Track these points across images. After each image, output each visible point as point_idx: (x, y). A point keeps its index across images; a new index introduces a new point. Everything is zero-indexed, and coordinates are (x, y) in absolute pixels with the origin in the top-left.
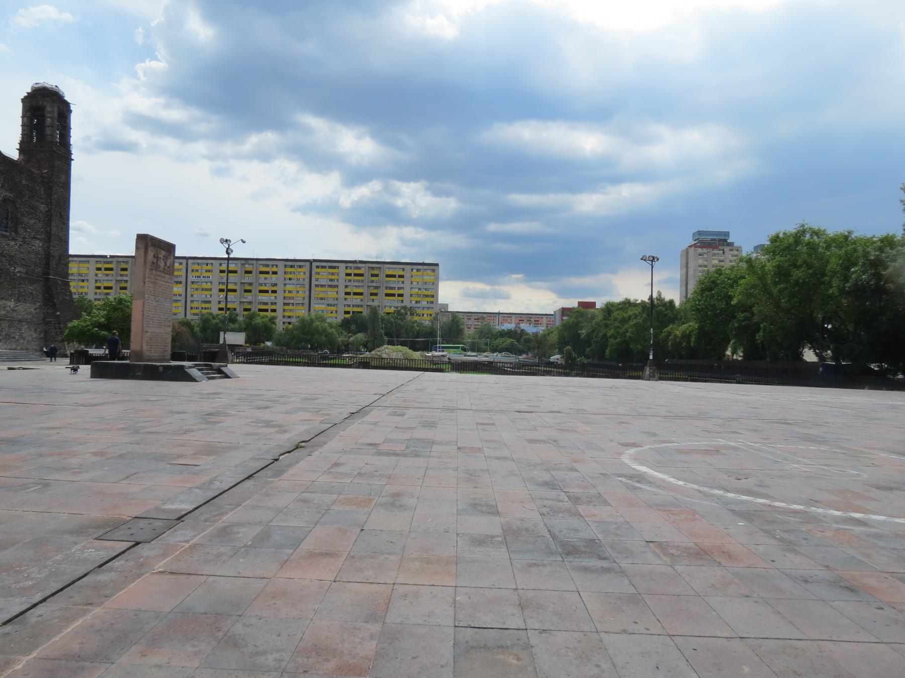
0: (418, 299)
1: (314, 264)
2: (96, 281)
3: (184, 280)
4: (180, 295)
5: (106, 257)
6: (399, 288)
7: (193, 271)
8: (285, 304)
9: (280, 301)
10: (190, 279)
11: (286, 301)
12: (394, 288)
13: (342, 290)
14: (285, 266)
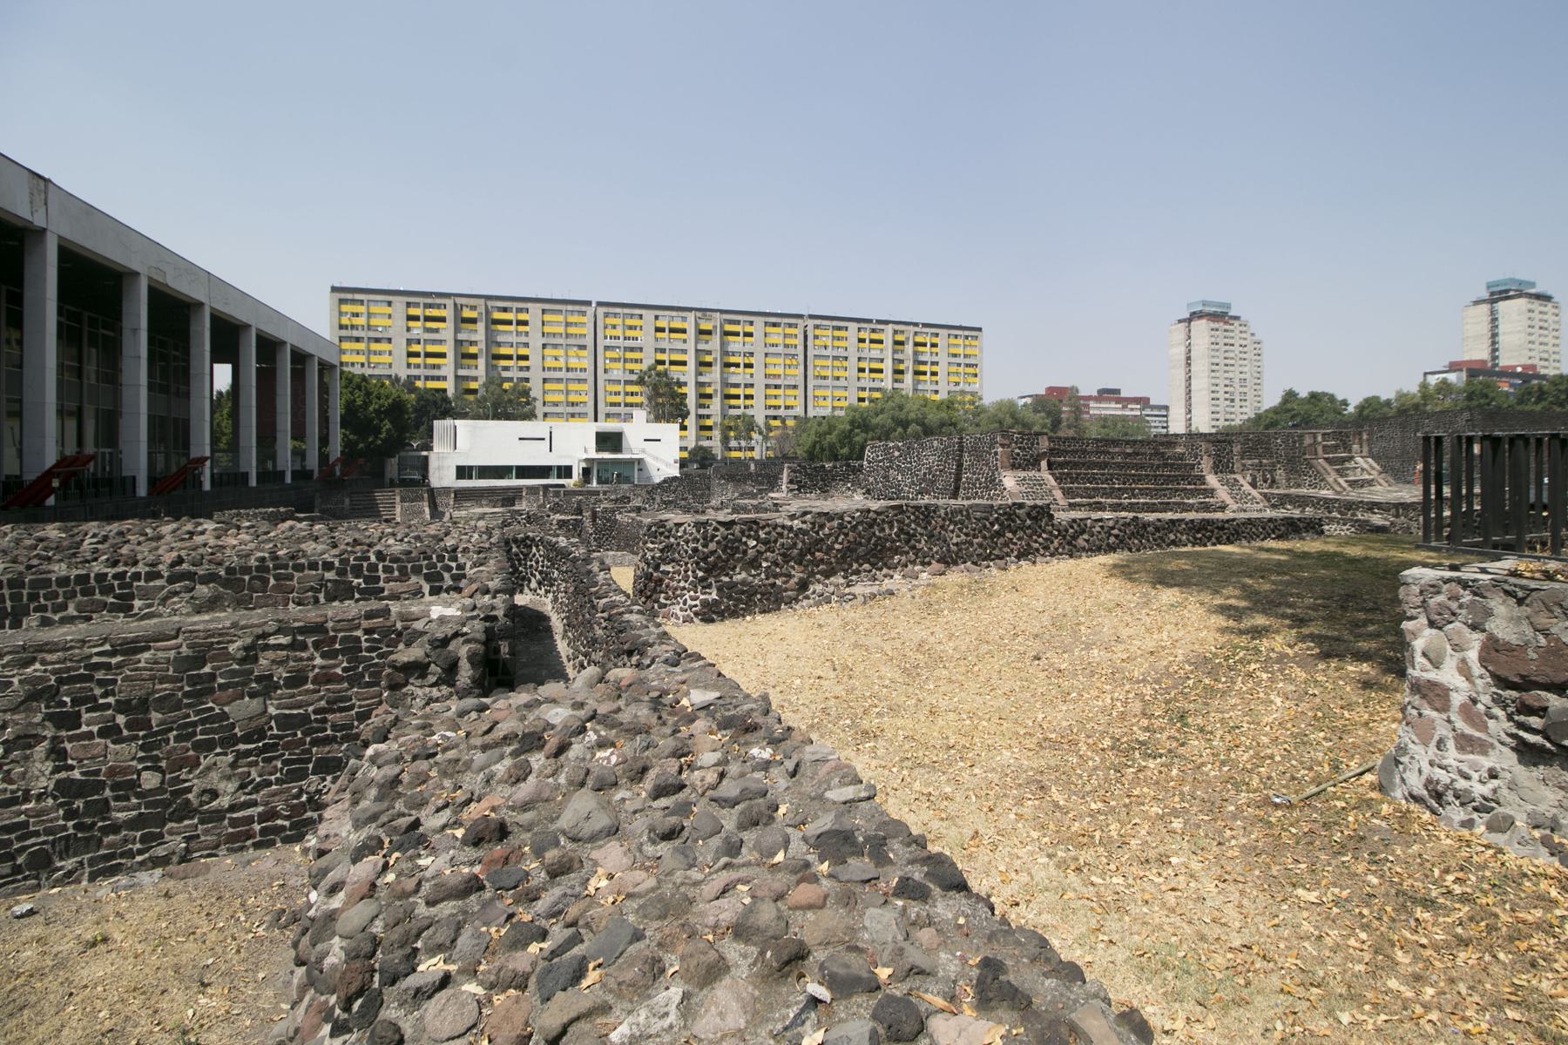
2: (409, 342)
3: (589, 341)
6: (934, 363)
8: (767, 386)
9: (759, 381)
10: (601, 343)
13: (853, 364)
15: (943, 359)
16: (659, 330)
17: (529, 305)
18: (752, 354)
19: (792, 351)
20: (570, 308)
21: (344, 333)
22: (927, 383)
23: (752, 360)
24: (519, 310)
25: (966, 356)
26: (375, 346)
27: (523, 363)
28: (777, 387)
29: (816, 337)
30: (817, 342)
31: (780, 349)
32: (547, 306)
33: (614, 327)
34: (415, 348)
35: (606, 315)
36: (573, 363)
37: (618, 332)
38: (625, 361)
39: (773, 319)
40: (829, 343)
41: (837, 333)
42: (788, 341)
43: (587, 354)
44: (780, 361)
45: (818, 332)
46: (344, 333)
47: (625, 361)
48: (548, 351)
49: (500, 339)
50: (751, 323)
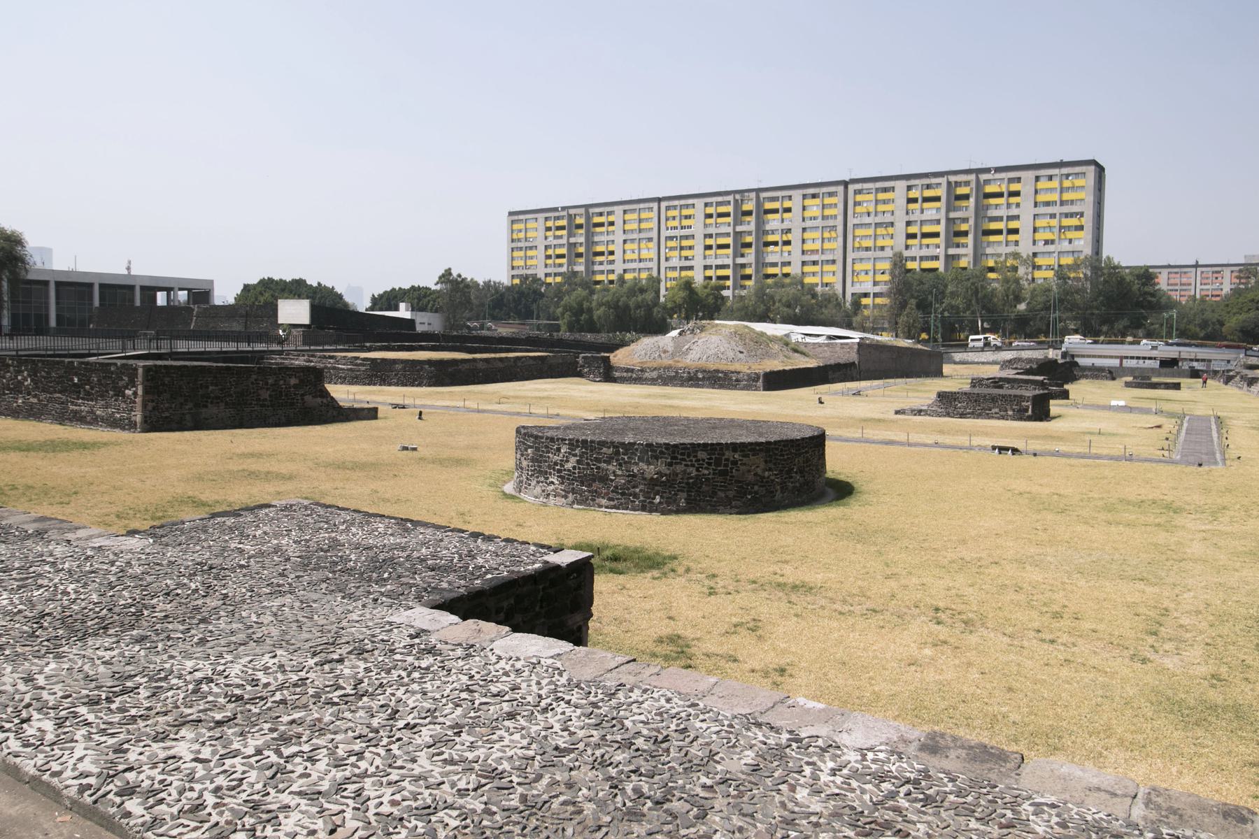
0: (1049, 236)
1: (851, 188)
3: (654, 234)
4: (651, 260)
5: (555, 209)
6: (1010, 218)
7: (667, 219)
8: (804, 263)
9: (796, 258)
10: (664, 233)
11: (807, 258)
12: (1000, 219)
14: (804, 197)
15: (1026, 210)
16: (911, 201)
17: (615, 208)
18: (789, 231)
19: (831, 223)
20: (642, 206)
21: (514, 245)
22: (998, 248)
23: (790, 237)
24: (609, 213)
25: (1062, 203)
26: (530, 253)
27: (611, 258)
28: (815, 263)
29: (856, 204)
30: (858, 209)
31: (819, 223)
32: (627, 207)
33: (674, 218)
34: (550, 252)
35: (668, 208)
36: (644, 254)
37: (676, 223)
38: (682, 248)
39: (811, 190)
40: (872, 209)
41: (881, 196)
42: (827, 212)
43: (653, 245)
44: (817, 235)
45: (859, 198)
46: (514, 245)
47: (682, 248)
48: (628, 246)
49: (596, 239)
50: (790, 198)
